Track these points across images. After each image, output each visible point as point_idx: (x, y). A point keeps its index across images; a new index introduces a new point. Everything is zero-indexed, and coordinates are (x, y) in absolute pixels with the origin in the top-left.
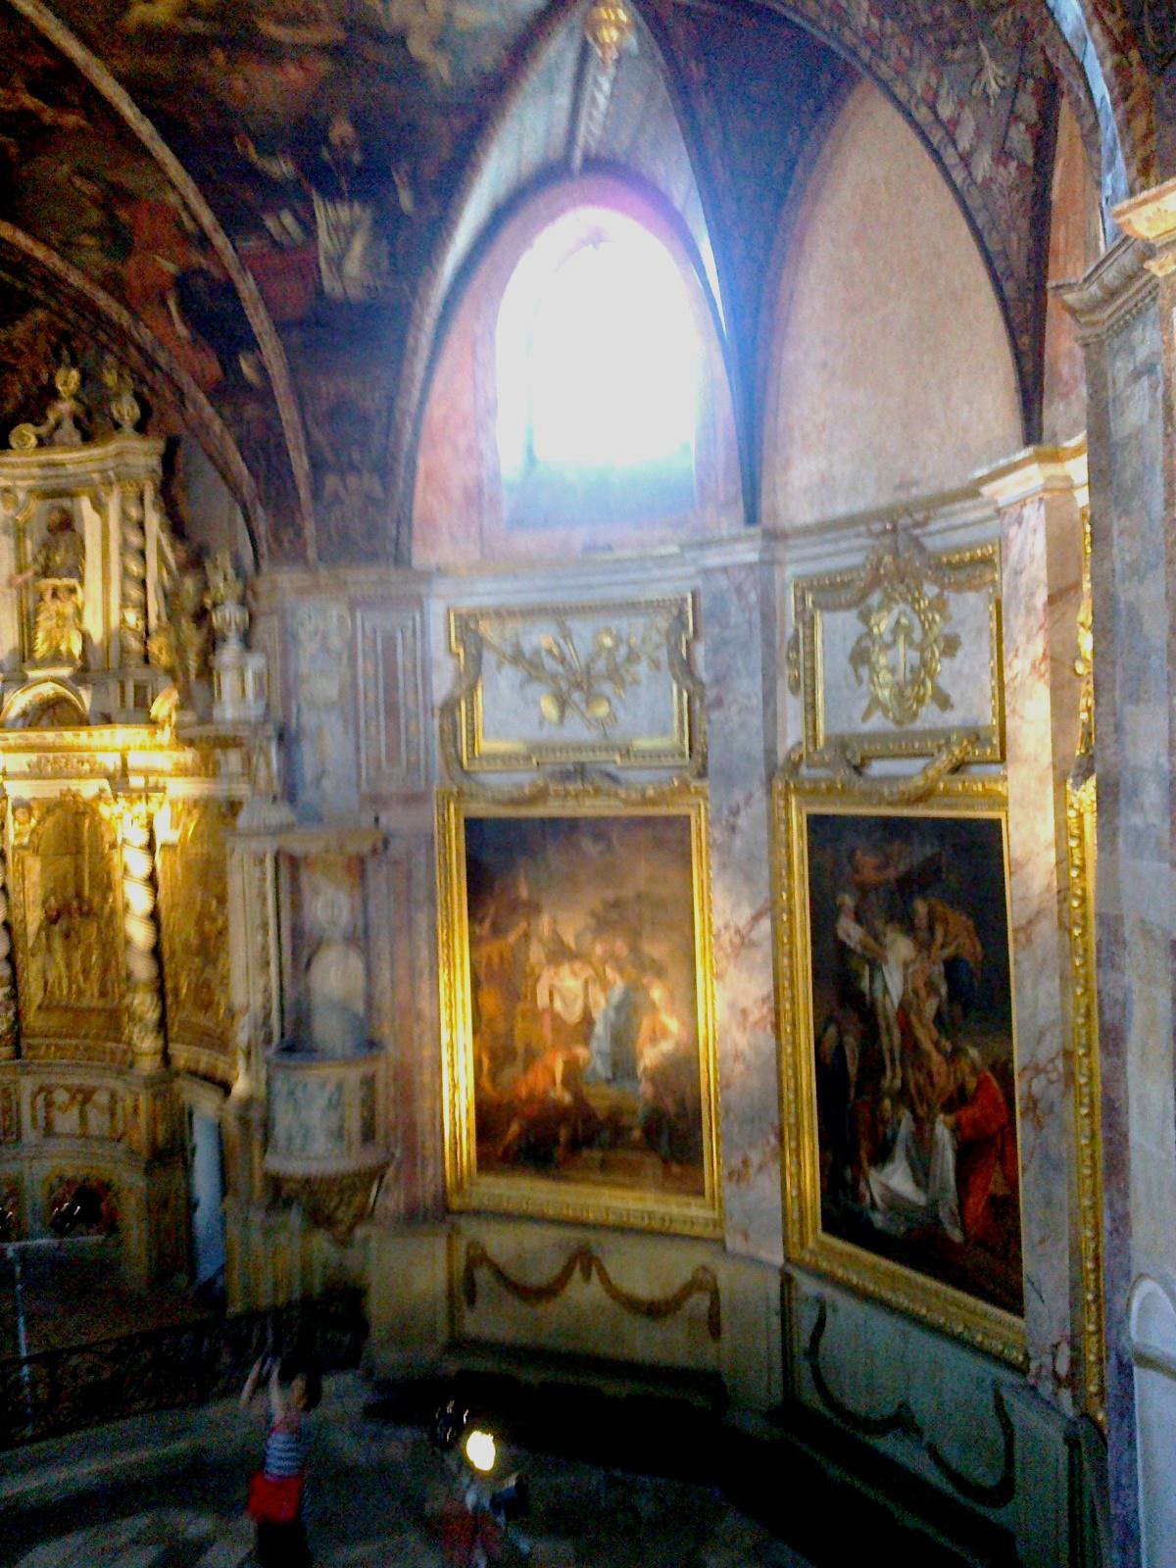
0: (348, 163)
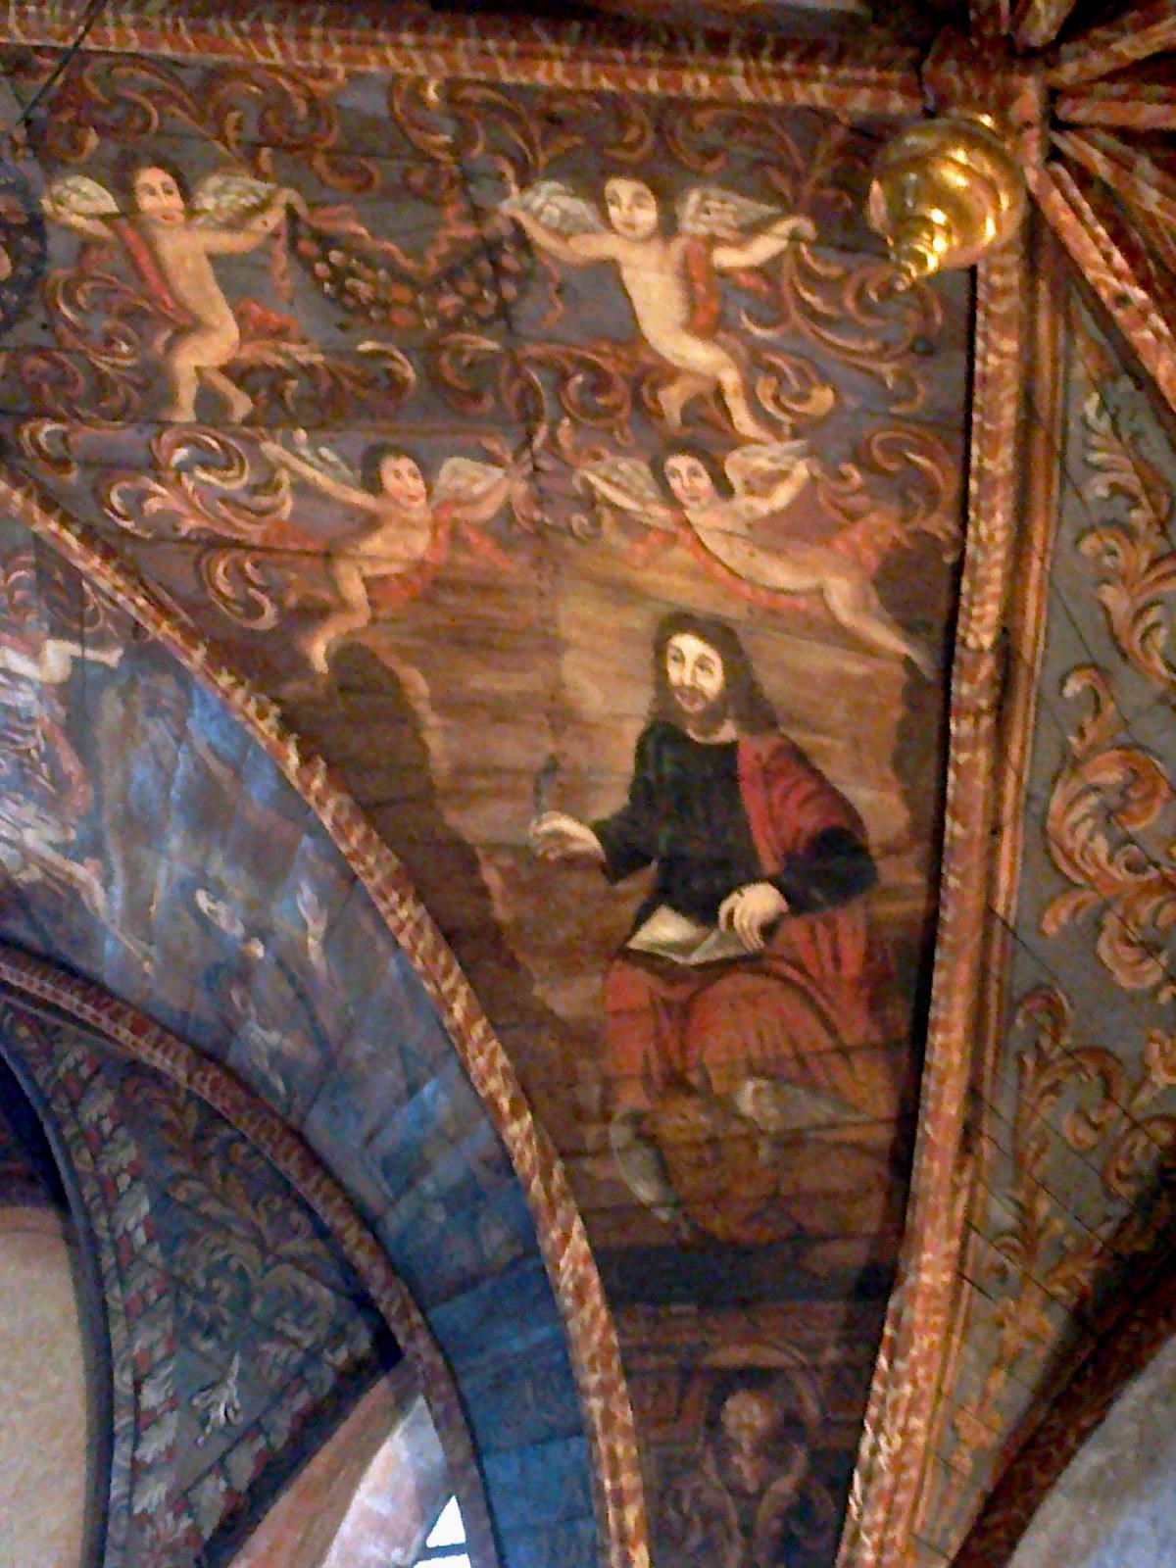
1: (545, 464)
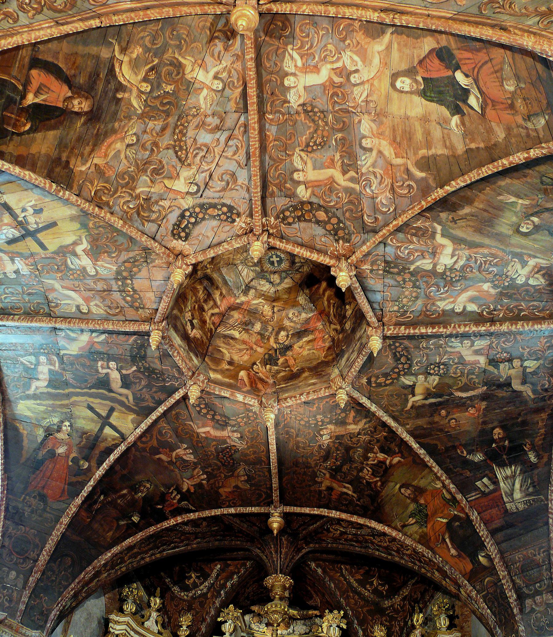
0: (504, 447)
1: (359, 110)
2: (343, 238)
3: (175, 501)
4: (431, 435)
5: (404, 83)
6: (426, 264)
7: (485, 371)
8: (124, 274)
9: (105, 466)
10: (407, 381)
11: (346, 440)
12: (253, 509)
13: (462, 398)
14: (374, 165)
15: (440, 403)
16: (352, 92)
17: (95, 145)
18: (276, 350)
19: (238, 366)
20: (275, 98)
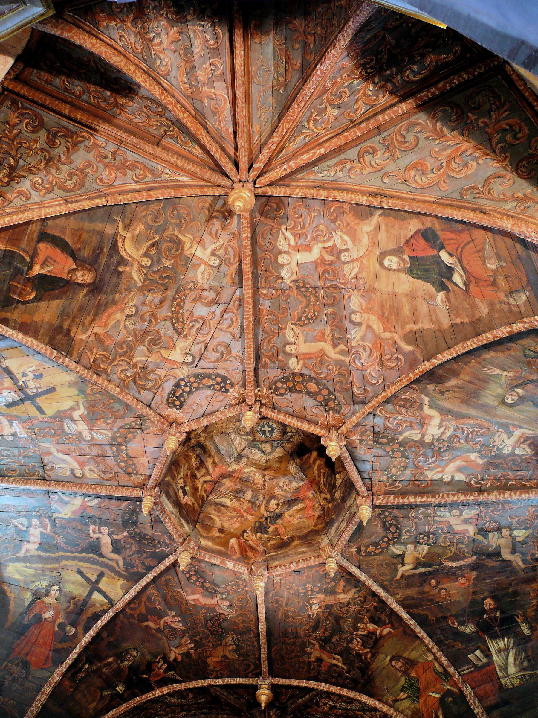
0: (496, 618)
1: (349, 287)
2: (333, 409)
3: (162, 671)
4: (422, 605)
5: (391, 262)
6: (414, 434)
7: (474, 540)
8: (119, 440)
9: (92, 632)
10: (397, 550)
11: (336, 611)
12: (241, 680)
13: (451, 568)
14: (363, 339)
15: (430, 573)
16: (342, 270)
17: (96, 315)
18: (266, 519)
19: (228, 534)
20: (269, 274)
